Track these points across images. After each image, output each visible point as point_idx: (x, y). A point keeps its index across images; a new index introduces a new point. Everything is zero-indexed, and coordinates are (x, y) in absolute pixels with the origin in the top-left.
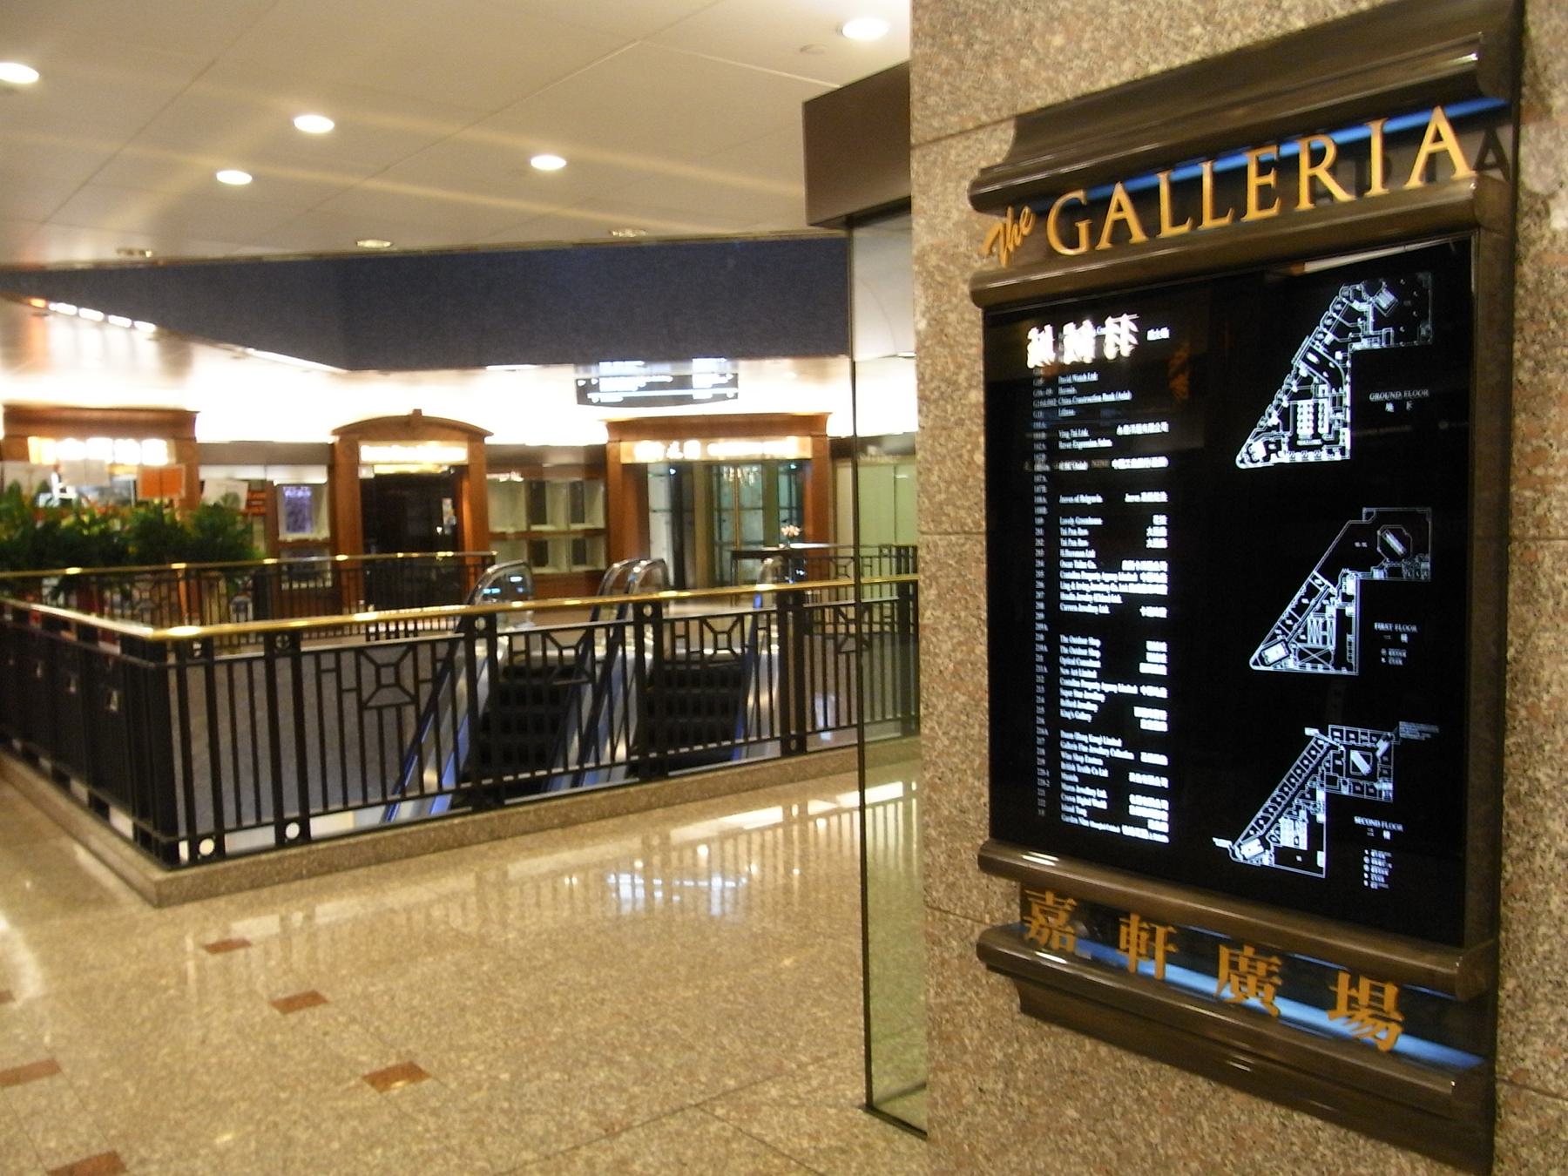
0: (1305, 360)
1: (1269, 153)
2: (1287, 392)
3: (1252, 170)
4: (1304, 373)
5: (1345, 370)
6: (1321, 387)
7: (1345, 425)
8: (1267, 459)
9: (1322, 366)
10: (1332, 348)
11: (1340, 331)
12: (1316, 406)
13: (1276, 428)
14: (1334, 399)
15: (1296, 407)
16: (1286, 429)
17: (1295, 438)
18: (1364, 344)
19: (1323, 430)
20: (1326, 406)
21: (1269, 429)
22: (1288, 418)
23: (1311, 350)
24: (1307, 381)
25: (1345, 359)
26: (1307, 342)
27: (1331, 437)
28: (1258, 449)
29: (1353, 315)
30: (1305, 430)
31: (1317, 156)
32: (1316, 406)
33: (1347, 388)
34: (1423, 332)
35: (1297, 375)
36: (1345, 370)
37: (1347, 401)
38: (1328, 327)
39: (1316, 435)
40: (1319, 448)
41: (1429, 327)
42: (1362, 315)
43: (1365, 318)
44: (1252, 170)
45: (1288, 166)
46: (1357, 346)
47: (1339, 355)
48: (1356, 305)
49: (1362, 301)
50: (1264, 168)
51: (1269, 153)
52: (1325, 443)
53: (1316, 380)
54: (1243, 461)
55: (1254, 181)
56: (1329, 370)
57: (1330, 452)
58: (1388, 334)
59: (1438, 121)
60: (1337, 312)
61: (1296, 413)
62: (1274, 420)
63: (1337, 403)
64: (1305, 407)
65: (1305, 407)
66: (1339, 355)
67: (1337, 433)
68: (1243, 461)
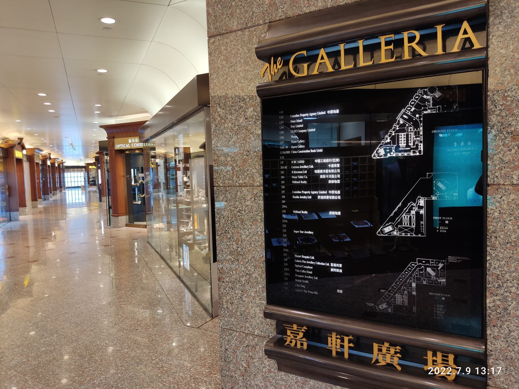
0: (402, 117)
1: (392, 37)
2: (394, 130)
3: (383, 44)
4: (401, 122)
5: (421, 121)
6: (410, 128)
7: (421, 142)
8: (385, 155)
9: (410, 120)
10: (414, 113)
11: (418, 106)
12: (407, 135)
13: (390, 143)
14: (415, 132)
15: (398, 135)
16: (394, 144)
17: (398, 147)
18: (429, 111)
19: (411, 144)
20: (412, 135)
21: (386, 144)
22: (395, 140)
23: (404, 114)
24: (404, 125)
25: (420, 117)
26: (403, 111)
27: (415, 147)
28: (382, 152)
29: (423, 100)
30: (402, 144)
31: (411, 39)
32: (407, 135)
33: (421, 128)
34: (455, 107)
35: (398, 124)
36: (421, 121)
37: (421, 133)
38: (413, 105)
39: (408, 146)
40: (409, 151)
41: (457, 105)
42: (428, 100)
43: (429, 102)
44: (383, 44)
45: (399, 43)
46: (425, 112)
47: (417, 116)
48: (425, 97)
49: (427, 95)
50: (387, 43)
51: (392, 37)
52: (412, 149)
53: (407, 125)
54: (375, 156)
55: (383, 47)
56: (413, 121)
57: (414, 152)
58: (439, 108)
59: (465, 25)
60: (417, 99)
61: (398, 138)
62: (389, 140)
63: (417, 134)
64: (402, 136)
65: (402, 136)
66: (417, 116)
67: (417, 145)
68: (375, 156)
